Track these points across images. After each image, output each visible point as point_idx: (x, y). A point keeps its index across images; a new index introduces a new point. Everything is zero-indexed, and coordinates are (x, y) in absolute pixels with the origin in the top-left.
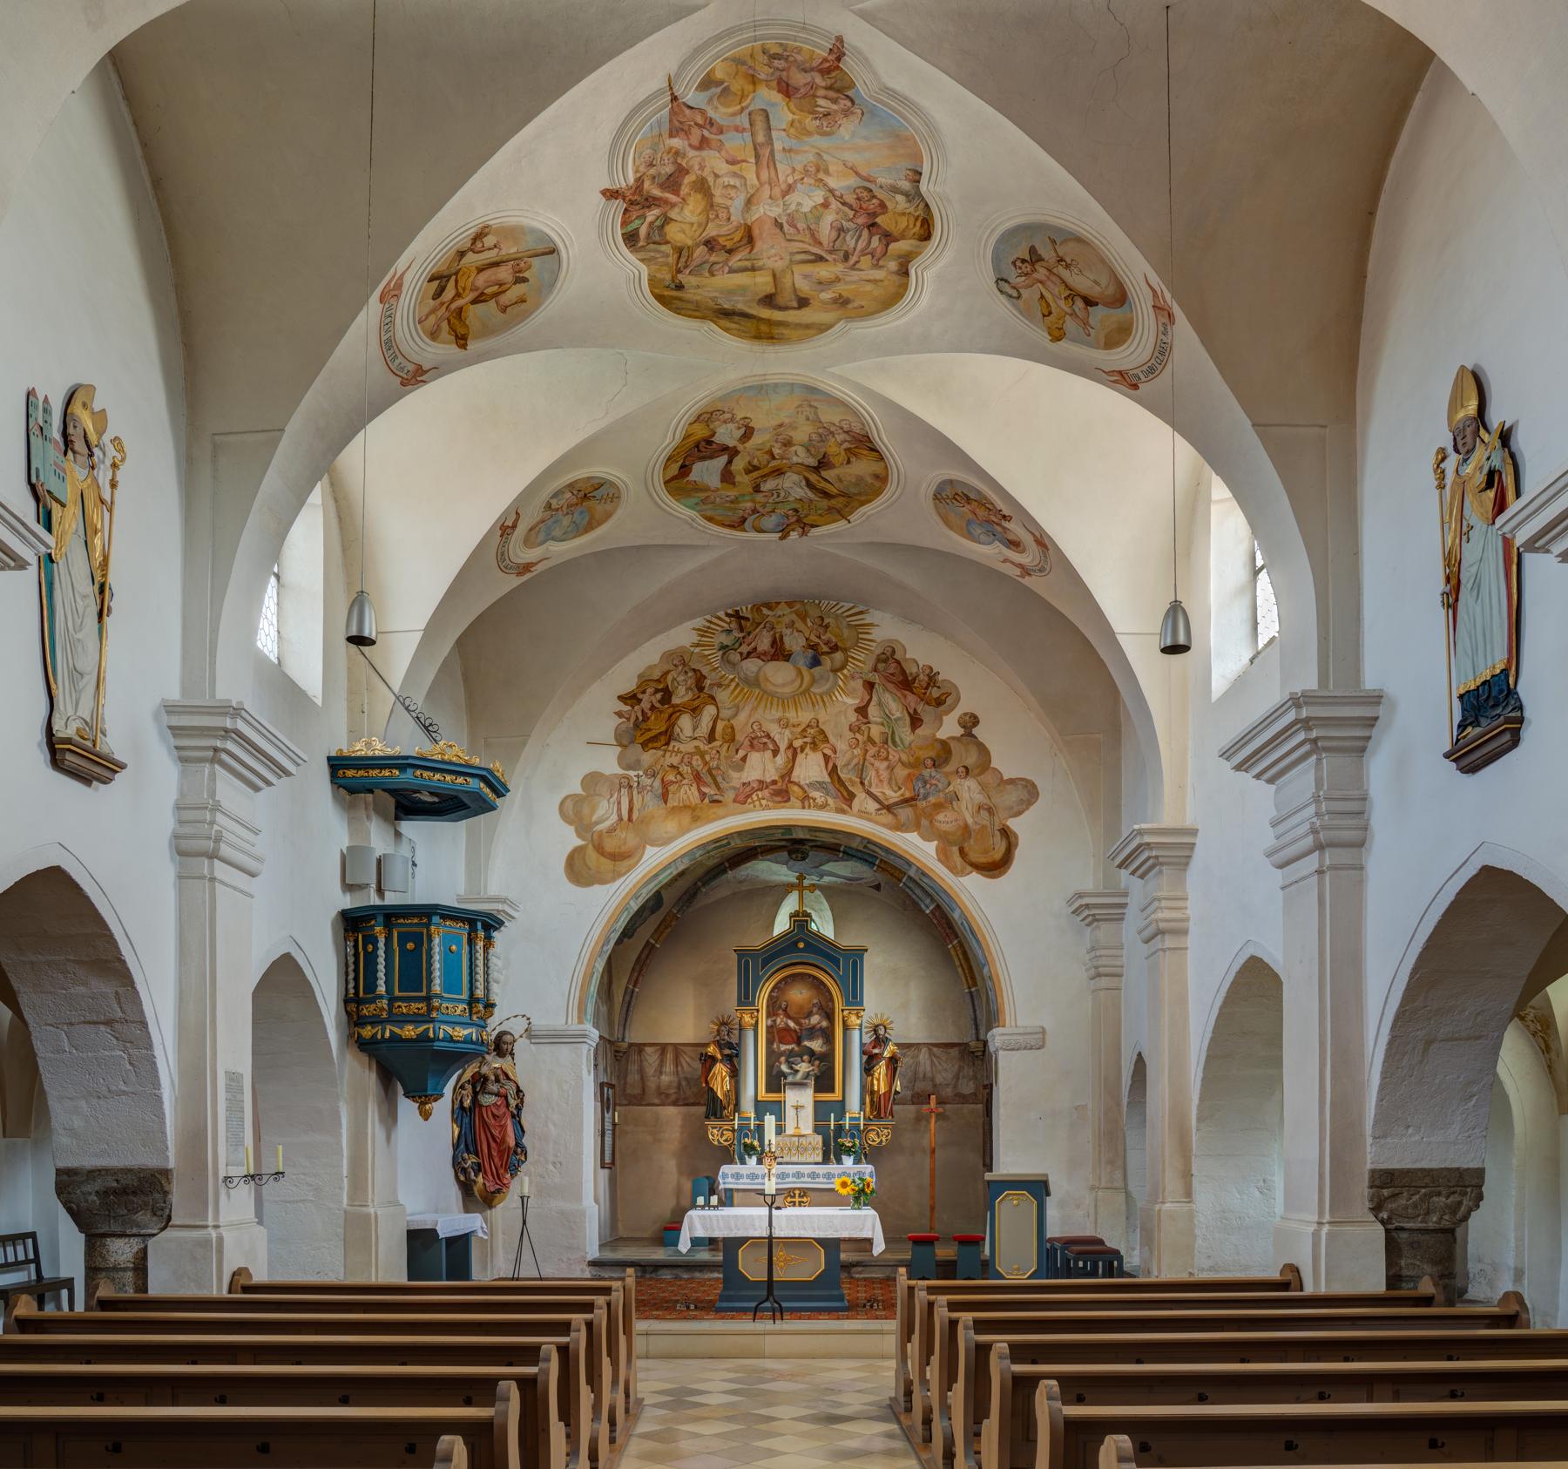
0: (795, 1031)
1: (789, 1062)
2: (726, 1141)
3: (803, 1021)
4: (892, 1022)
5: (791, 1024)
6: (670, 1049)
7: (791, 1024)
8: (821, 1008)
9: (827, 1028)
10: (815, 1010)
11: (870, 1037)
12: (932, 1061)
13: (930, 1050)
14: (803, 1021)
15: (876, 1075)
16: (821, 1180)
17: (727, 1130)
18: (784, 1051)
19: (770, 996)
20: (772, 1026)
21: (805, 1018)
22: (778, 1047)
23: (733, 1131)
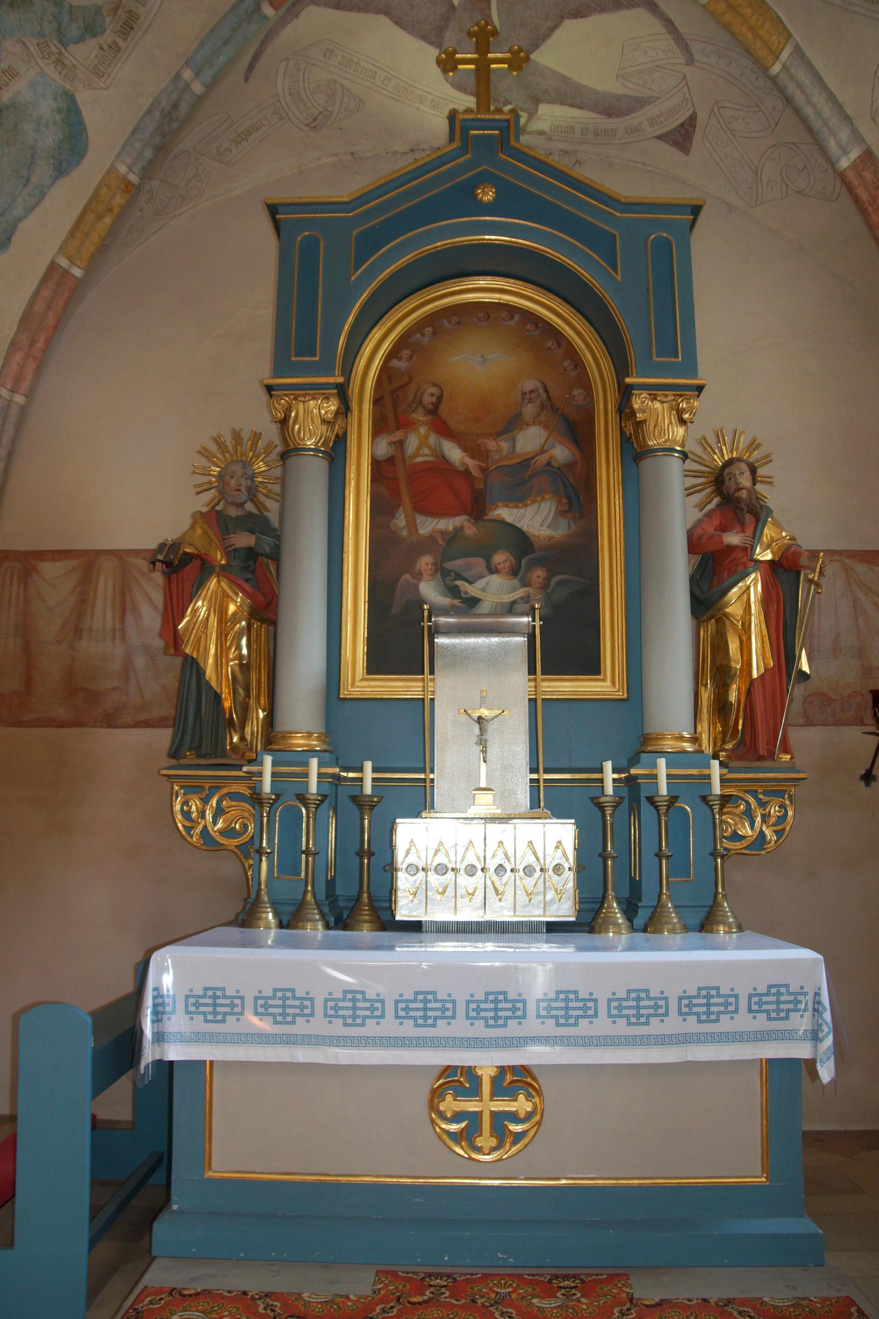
0: (467, 473)
1: (444, 575)
2: (228, 832)
3: (491, 445)
4: (767, 460)
5: (454, 453)
6: (108, 566)
7: (454, 453)
8: (549, 405)
9: (570, 465)
10: (529, 410)
11: (701, 506)
12: (855, 601)
13: (847, 569)
14: (491, 445)
15: (734, 609)
16: (602, 1026)
17: (235, 796)
18: (431, 538)
19: (385, 369)
20: (391, 460)
21: (497, 435)
22: (412, 526)
23: (256, 799)
